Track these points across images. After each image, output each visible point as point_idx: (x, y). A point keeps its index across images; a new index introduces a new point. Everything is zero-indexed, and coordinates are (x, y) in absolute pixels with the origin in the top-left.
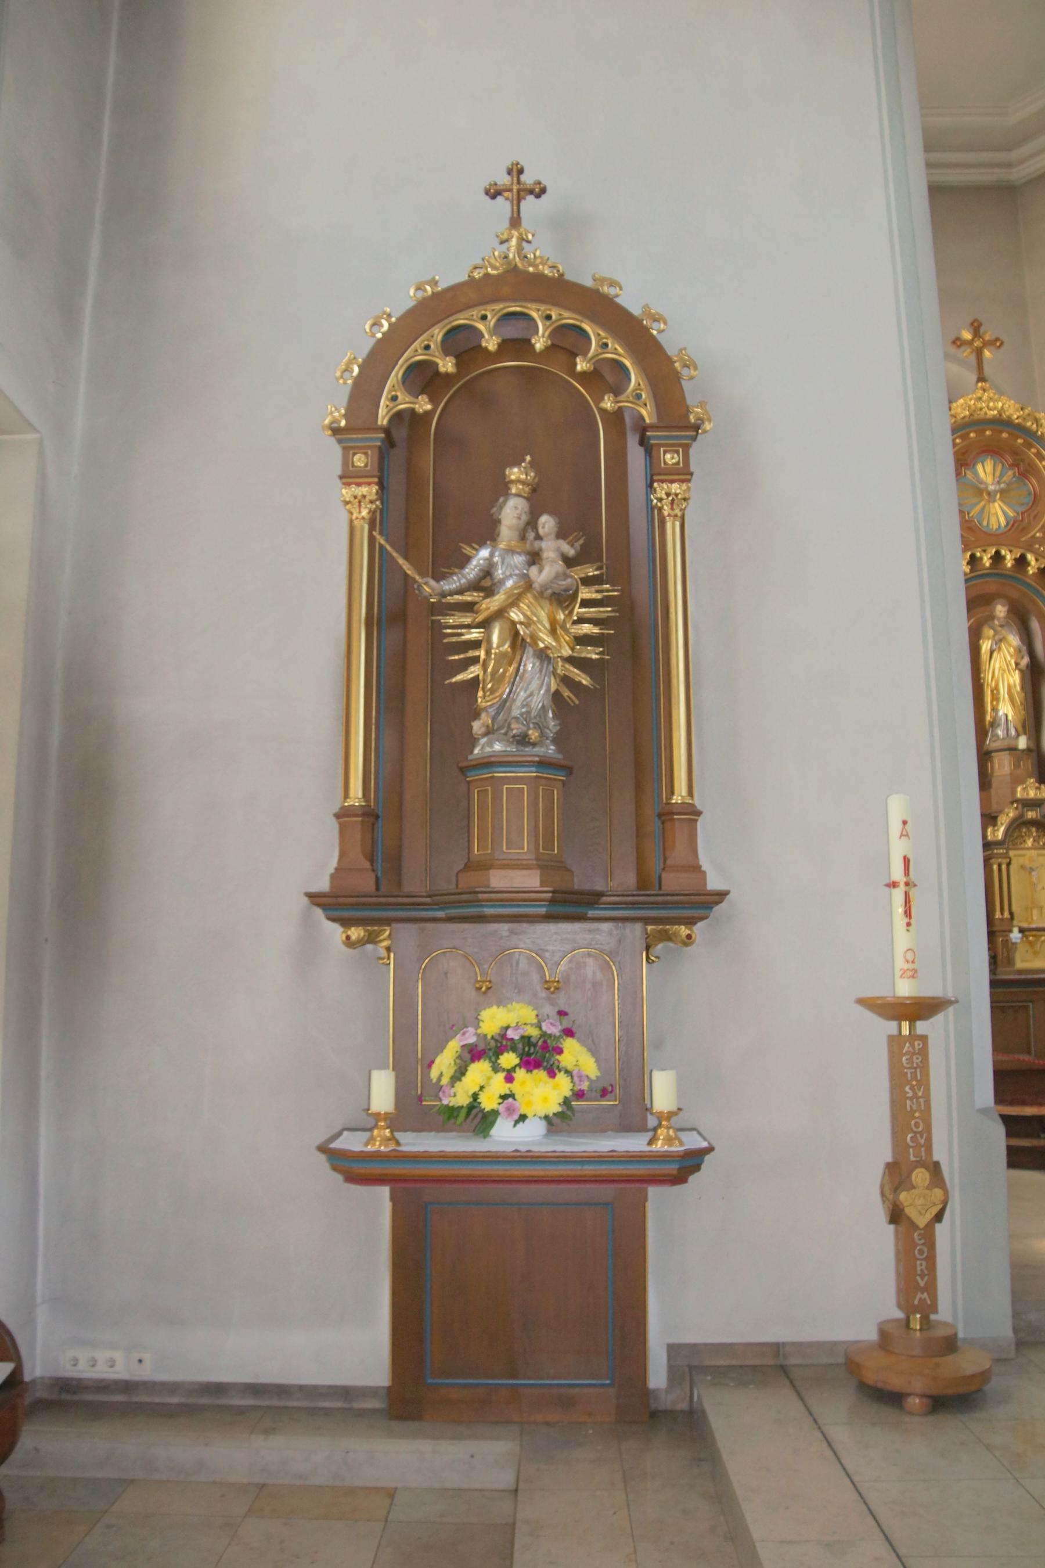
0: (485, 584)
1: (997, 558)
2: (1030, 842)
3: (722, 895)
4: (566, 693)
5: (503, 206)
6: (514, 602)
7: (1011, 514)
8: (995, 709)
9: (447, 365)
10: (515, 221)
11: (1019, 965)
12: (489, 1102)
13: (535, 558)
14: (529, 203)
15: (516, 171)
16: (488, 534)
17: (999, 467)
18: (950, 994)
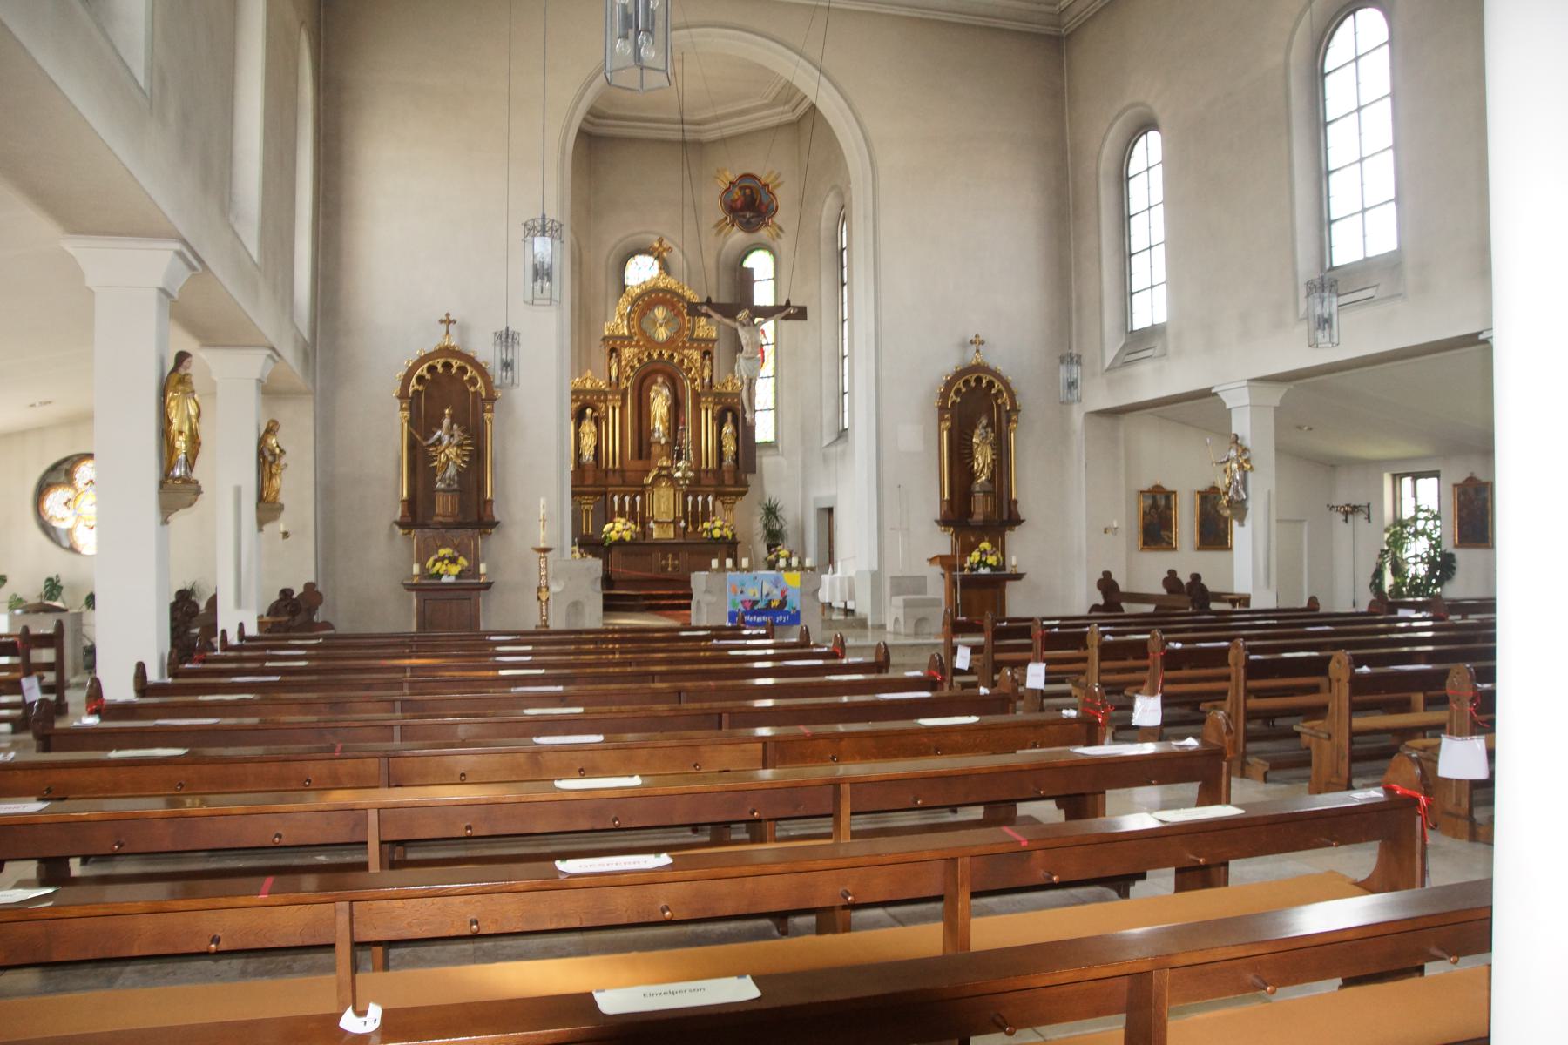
0: (440, 440)
1: (661, 355)
2: (664, 484)
3: (498, 523)
5: (444, 326)
6: (447, 447)
8: (654, 424)
10: (448, 332)
11: (655, 536)
12: (441, 572)
13: (452, 436)
14: (451, 325)
16: (440, 427)
17: (665, 310)
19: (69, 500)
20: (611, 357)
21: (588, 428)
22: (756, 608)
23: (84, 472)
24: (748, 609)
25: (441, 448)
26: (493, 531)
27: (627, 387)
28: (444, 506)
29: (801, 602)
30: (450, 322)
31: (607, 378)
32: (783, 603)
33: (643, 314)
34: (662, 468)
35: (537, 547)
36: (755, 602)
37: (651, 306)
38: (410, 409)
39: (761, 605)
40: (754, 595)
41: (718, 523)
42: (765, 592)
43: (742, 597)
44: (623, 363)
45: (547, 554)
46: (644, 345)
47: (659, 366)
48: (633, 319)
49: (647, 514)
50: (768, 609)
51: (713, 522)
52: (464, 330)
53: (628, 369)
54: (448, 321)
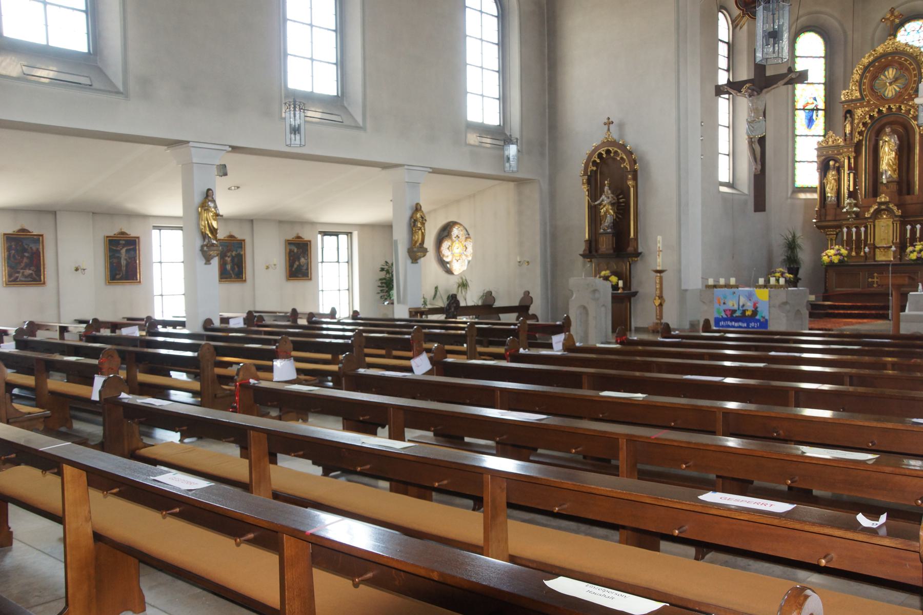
1: (890, 109)
3: (640, 253)
4: (617, 220)
5: (607, 126)
7: (898, 89)
9: (598, 161)
13: (608, 198)
14: (611, 125)
15: (605, 124)
17: (895, 70)
18: (665, 269)
19: (450, 246)
20: (846, 118)
21: (831, 175)
22: (734, 315)
23: (455, 231)
24: (729, 316)
25: (602, 207)
26: (639, 258)
27: (860, 142)
28: (605, 245)
29: (769, 313)
30: (610, 124)
31: (842, 133)
32: (755, 312)
33: (875, 77)
34: (881, 203)
35: (655, 269)
36: (734, 311)
37: (884, 68)
38: (589, 182)
39: (738, 314)
40: (733, 305)
41: (918, 248)
42: (741, 304)
43: (725, 307)
44: (856, 121)
45: (662, 274)
46: (874, 103)
47: (884, 121)
48: (864, 84)
49: (869, 242)
50: (743, 318)
51: (914, 246)
52: (621, 126)
53: (861, 125)
54: (609, 123)
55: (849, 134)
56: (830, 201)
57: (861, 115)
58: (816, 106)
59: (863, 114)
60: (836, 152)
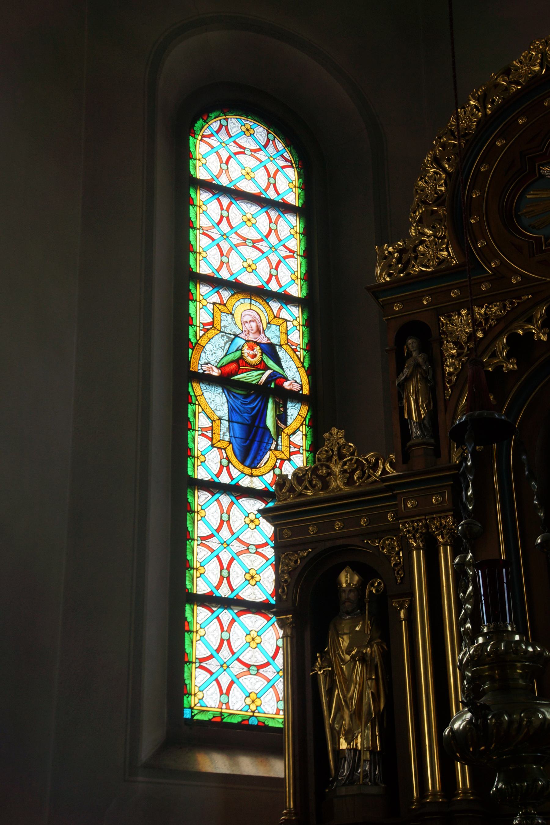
55: (420, 423)
56: (352, 779)
57: (472, 336)
58: (274, 376)
59: (480, 335)
60: (363, 522)
